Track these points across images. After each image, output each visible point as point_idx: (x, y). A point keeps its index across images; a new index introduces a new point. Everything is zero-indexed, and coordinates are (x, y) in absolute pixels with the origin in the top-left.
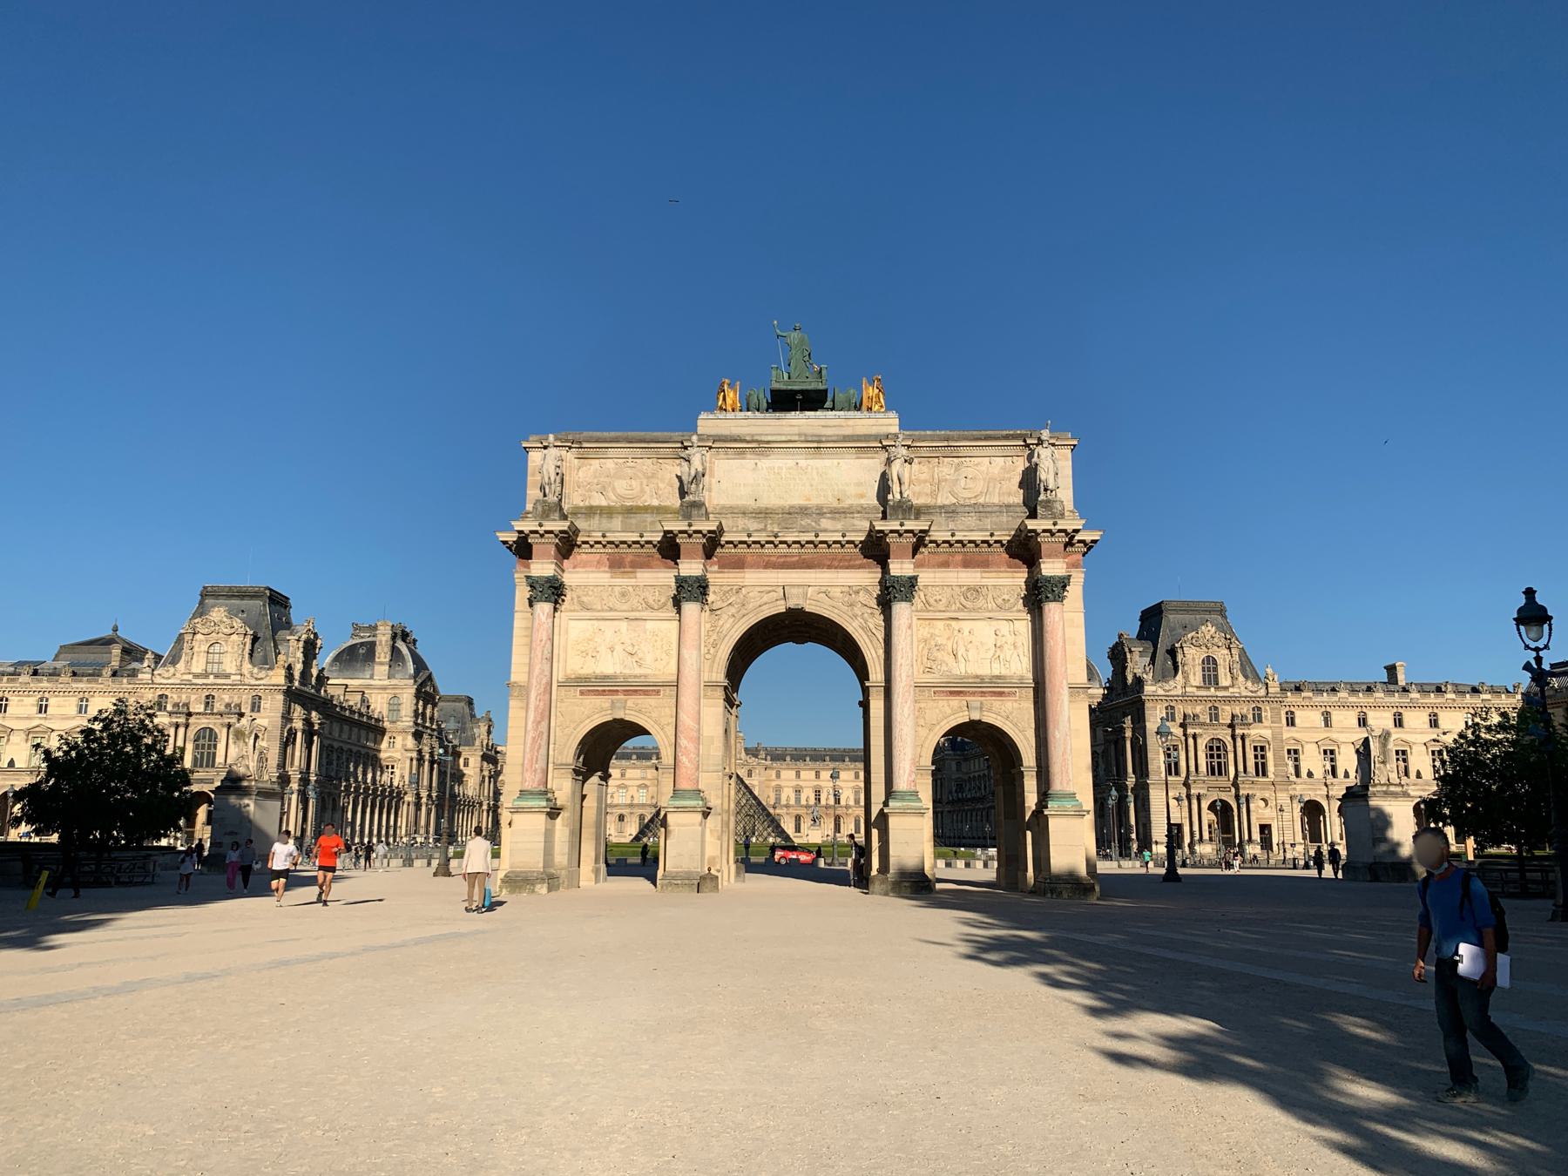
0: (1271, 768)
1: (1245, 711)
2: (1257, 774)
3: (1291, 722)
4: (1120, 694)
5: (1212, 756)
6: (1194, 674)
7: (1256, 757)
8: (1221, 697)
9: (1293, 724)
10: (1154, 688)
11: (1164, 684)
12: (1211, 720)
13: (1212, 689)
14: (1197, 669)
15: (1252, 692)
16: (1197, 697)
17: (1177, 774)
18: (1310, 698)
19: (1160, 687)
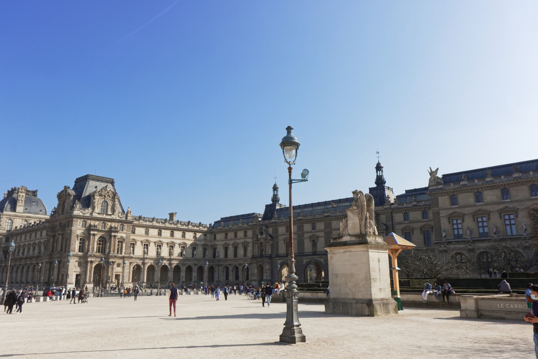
0: (124, 250)
1: (116, 226)
2: (118, 253)
3: (134, 232)
4: (60, 214)
5: (100, 244)
6: (98, 208)
7: (118, 245)
8: (108, 219)
9: (134, 233)
10: (78, 212)
11: (83, 210)
12: (102, 228)
13: (104, 215)
14: (99, 206)
15: (120, 218)
16: (98, 218)
17: (82, 252)
18: (142, 223)
19: (81, 212)
